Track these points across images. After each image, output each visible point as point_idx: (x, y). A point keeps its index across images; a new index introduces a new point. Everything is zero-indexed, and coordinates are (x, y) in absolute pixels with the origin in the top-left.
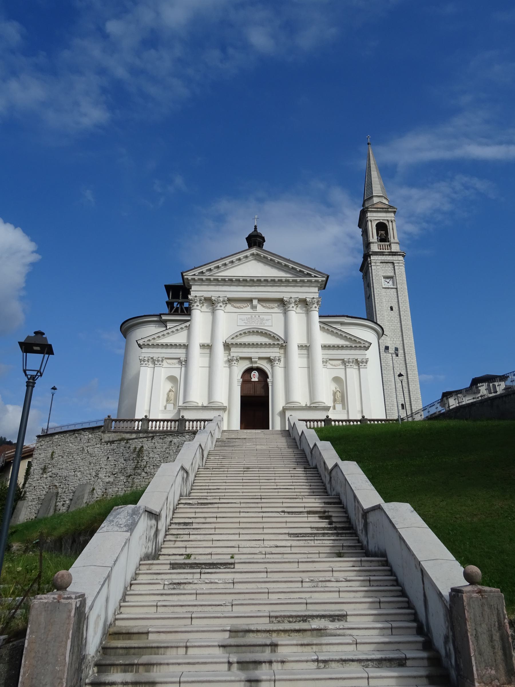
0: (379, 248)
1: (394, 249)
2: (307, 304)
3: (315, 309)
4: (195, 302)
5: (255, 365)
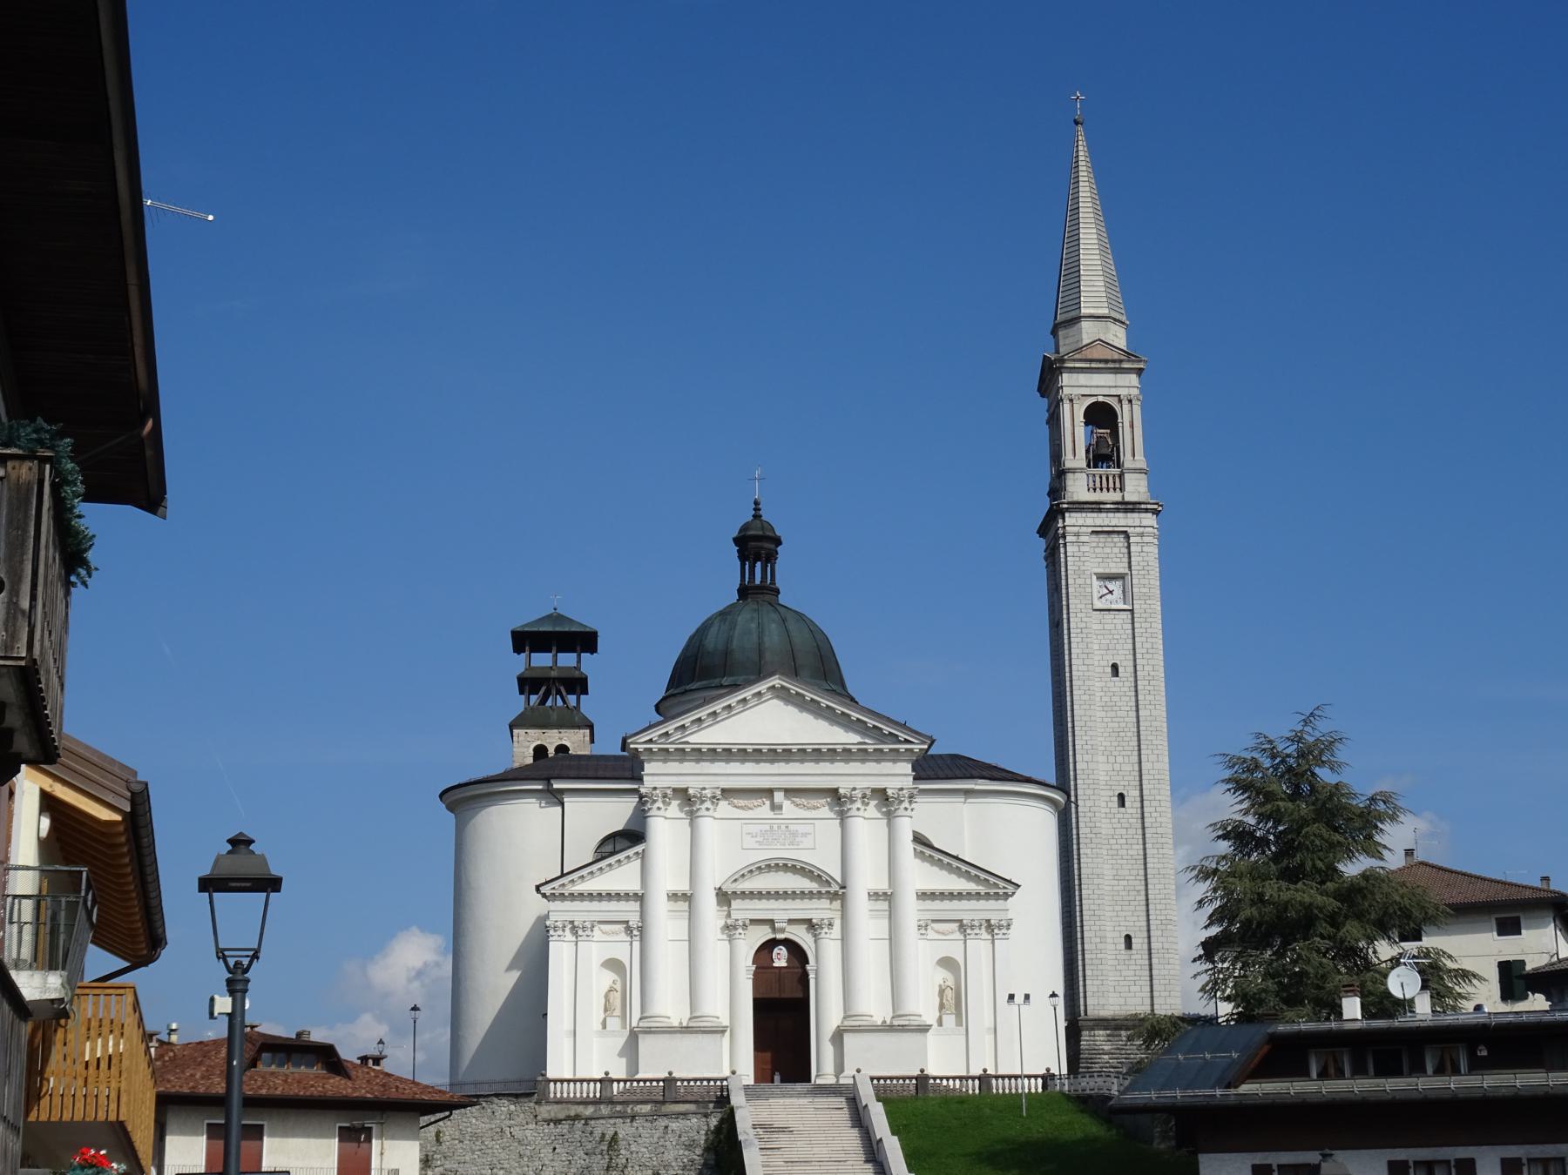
0: (1091, 485)
4: (655, 801)
5: (780, 936)
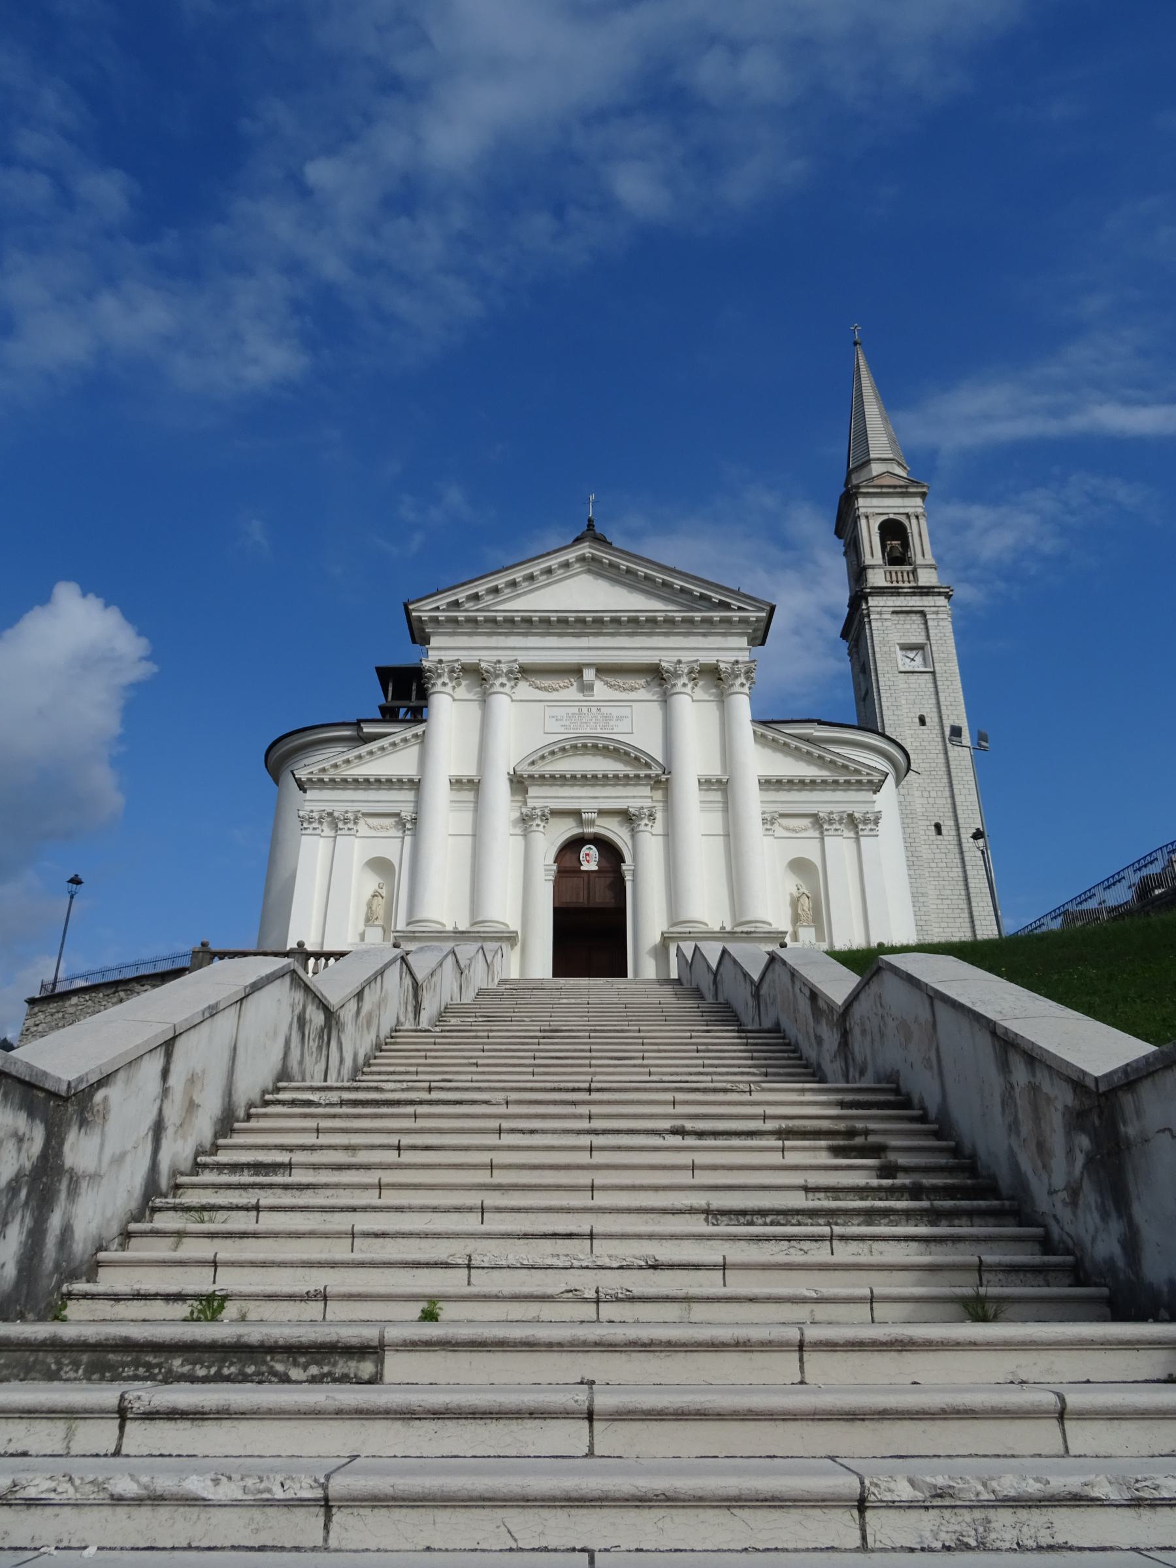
0: (888, 578)
1: (925, 580)
2: (720, 679)
3: (741, 690)
4: (440, 676)
5: (589, 830)
